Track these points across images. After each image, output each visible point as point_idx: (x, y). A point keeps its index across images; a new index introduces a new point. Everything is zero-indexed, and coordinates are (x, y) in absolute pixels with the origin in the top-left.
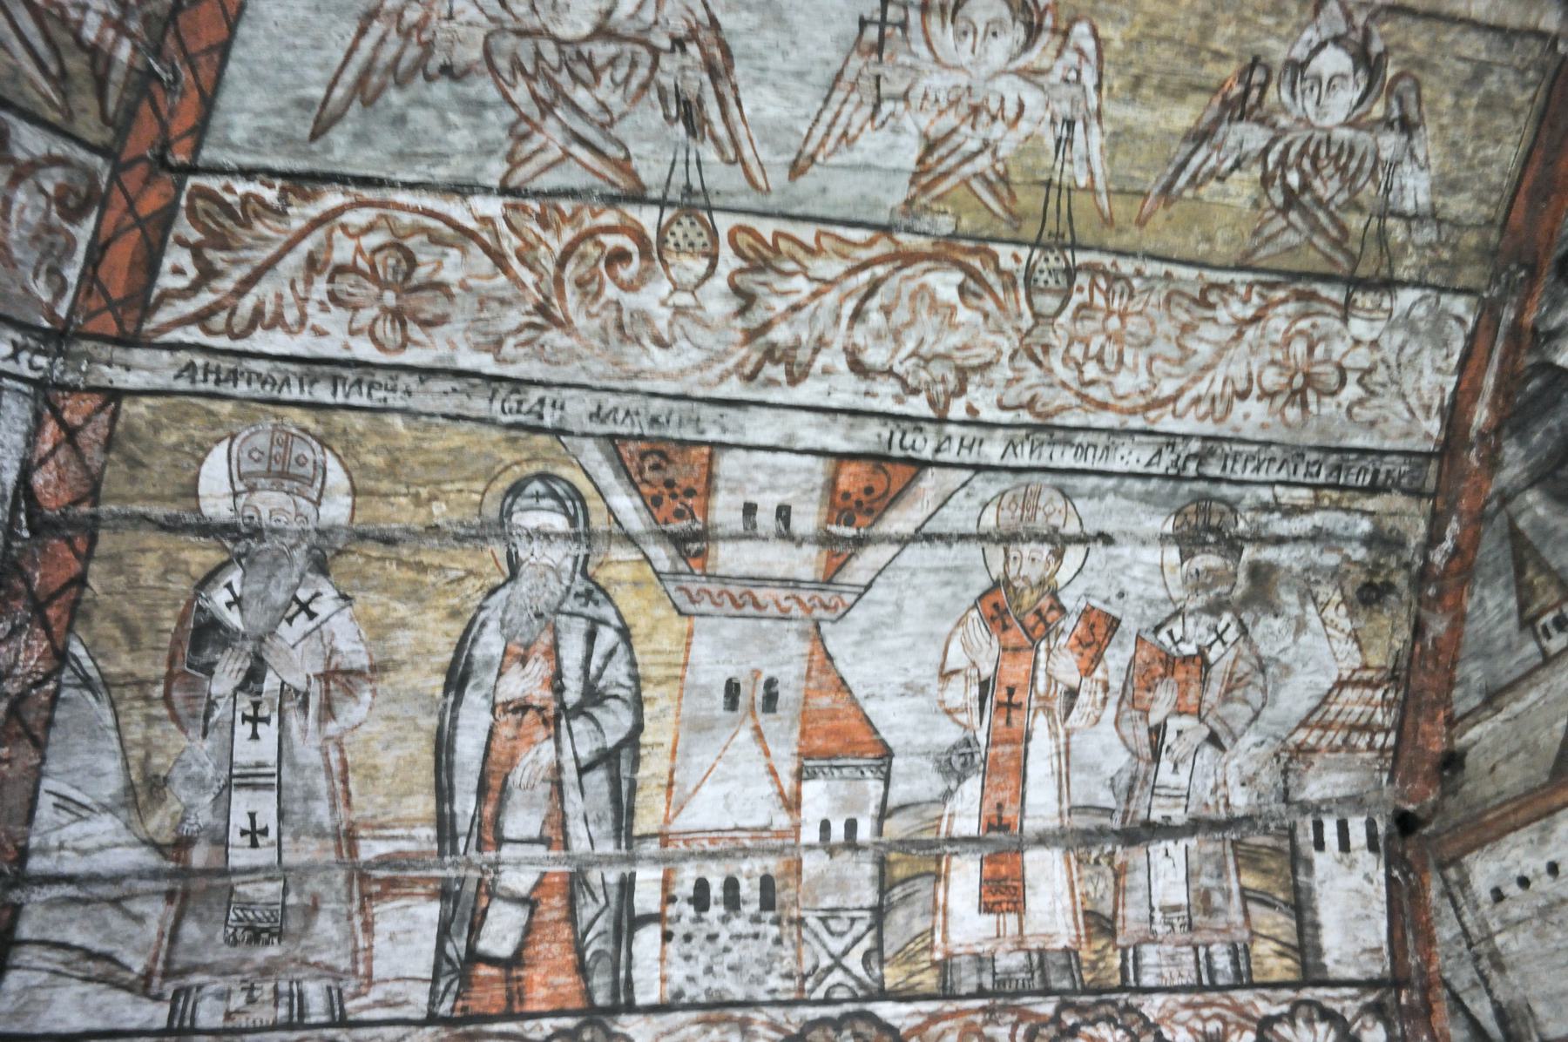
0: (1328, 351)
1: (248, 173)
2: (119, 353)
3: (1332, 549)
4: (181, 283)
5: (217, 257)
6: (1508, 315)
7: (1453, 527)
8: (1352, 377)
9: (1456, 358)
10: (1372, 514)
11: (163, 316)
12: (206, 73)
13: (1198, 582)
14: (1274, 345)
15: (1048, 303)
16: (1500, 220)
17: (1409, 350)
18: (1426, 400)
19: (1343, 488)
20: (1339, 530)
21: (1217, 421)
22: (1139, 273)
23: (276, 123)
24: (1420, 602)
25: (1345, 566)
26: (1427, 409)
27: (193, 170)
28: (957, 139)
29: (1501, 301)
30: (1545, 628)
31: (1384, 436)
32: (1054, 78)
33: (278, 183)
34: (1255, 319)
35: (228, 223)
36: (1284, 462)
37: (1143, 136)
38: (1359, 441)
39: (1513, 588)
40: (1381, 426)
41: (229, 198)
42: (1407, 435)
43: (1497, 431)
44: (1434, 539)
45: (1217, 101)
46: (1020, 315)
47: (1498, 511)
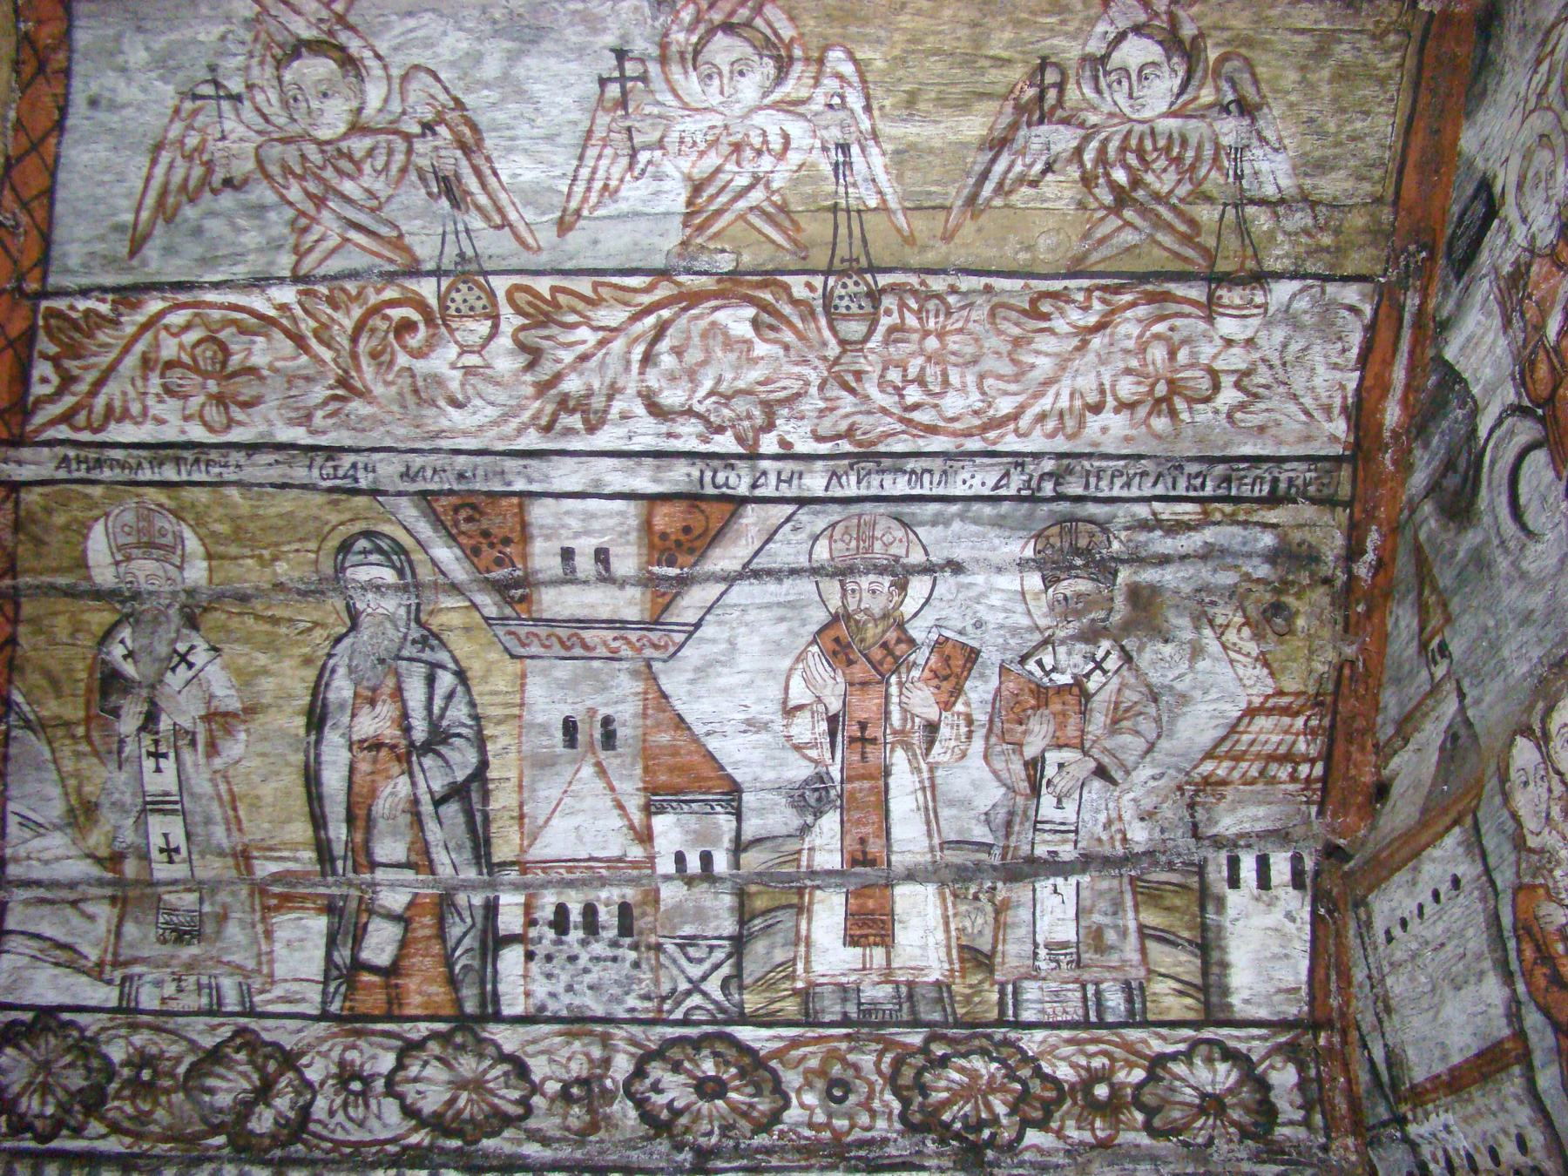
0: (1192, 354)
1: (85, 292)
2: (12, 452)
4: (47, 390)
5: (71, 365)
6: (1412, 302)
7: (1373, 538)
8: (1227, 381)
9: (1355, 351)
10: (1274, 526)
11: (39, 419)
12: (40, 215)
13: (1067, 608)
14: (1127, 351)
15: (855, 329)
17: (1294, 347)
18: (1325, 401)
19: (1238, 500)
20: (1236, 545)
21: (1069, 437)
22: (953, 290)
23: (99, 247)
25: (1246, 585)
26: (1327, 409)
27: (45, 294)
28: (724, 177)
29: (1402, 284)
32: (818, 105)
33: (110, 297)
34: (1100, 327)
35: (77, 336)
36: (1159, 476)
37: (931, 151)
38: (1248, 450)
40: (1273, 431)
41: (74, 315)
45: (1009, 107)
46: (825, 344)
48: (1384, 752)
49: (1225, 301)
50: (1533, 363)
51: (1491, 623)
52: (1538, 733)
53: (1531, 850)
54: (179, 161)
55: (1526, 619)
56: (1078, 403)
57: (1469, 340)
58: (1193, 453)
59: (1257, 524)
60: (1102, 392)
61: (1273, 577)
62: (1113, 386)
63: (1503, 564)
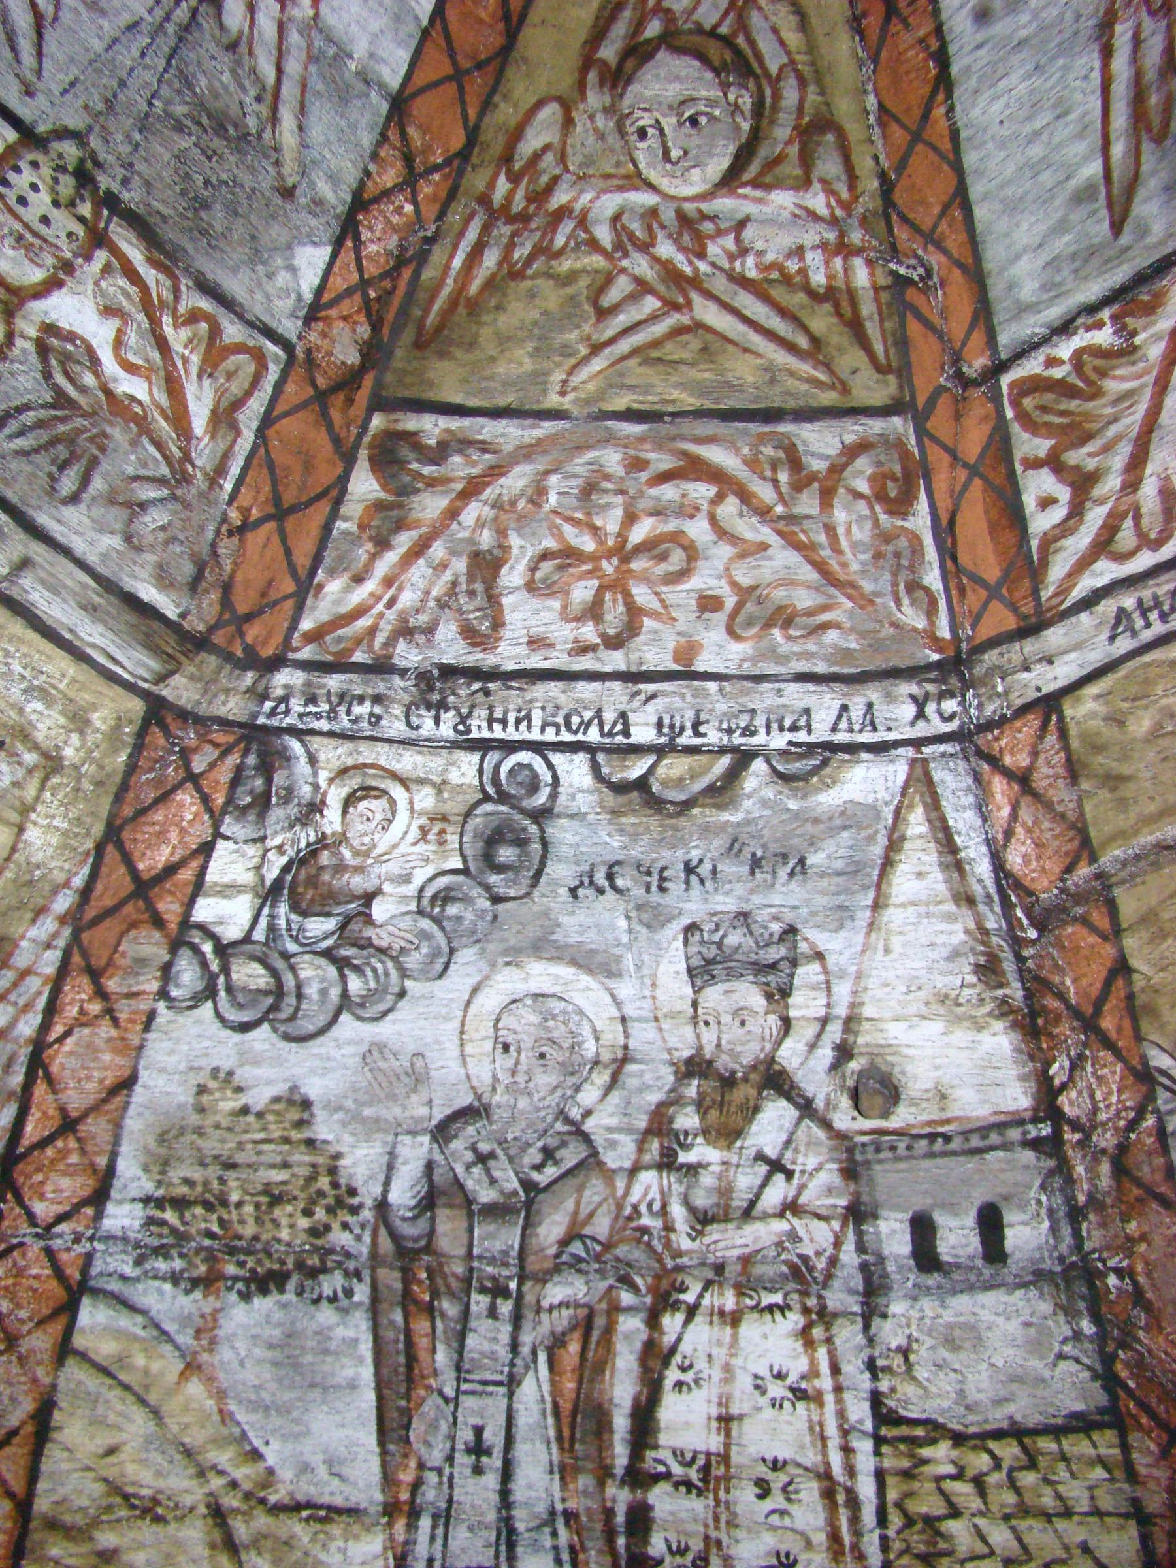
1: (1064, 328)
2: (1030, 646)
4: (1058, 514)
5: (1081, 457)
11: (1057, 571)
12: (955, 241)
23: (1063, 243)
27: (1002, 367)
33: (1105, 314)
35: (1073, 405)
41: (1058, 373)
54: (1148, 24)
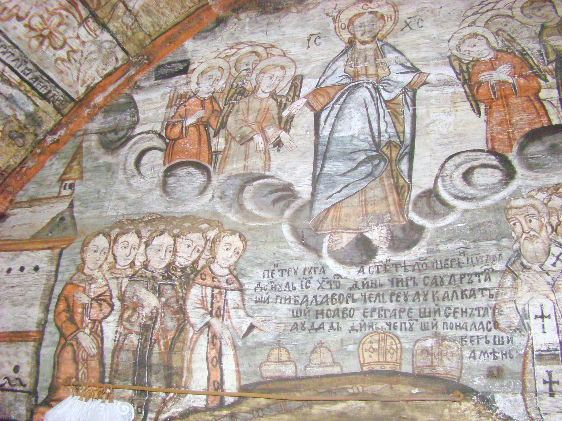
0: (65, 31)
3: (12, 108)
6: (132, 72)
7: (62, 132)
8: (67, 48)
9: (106, 72)
10: (37, 106)
14: (47, 10)
16: (153, 38)
17: (93, 56)
18: (86, 79)
19: (34, 88)
20: (20, 102)
24: (31, 152)
25: (12, 118)
26: (84, 82)
29: (134, 65)
30: (66, 184)
31: (62, 81)
36: (18, 59)
38: (51, 75)
39: (66, 166)
40: (64, 75)
42: (71, 86)
43: (100, 108)
44: (53, 132)
47: (80, 135)
48: (13, 204)
49: (89, 24)
50: (174, 125)
51: (103, 191)
52: (112, 238)
53: (84, 274)
55: (123, 198)
56: (15, 11)
57: (149, 99)
58: (35, 61)
59: (33, 101)
60: (27, 15)
61: (23, 122)
62: (32, 17)
63: (121, 176)
